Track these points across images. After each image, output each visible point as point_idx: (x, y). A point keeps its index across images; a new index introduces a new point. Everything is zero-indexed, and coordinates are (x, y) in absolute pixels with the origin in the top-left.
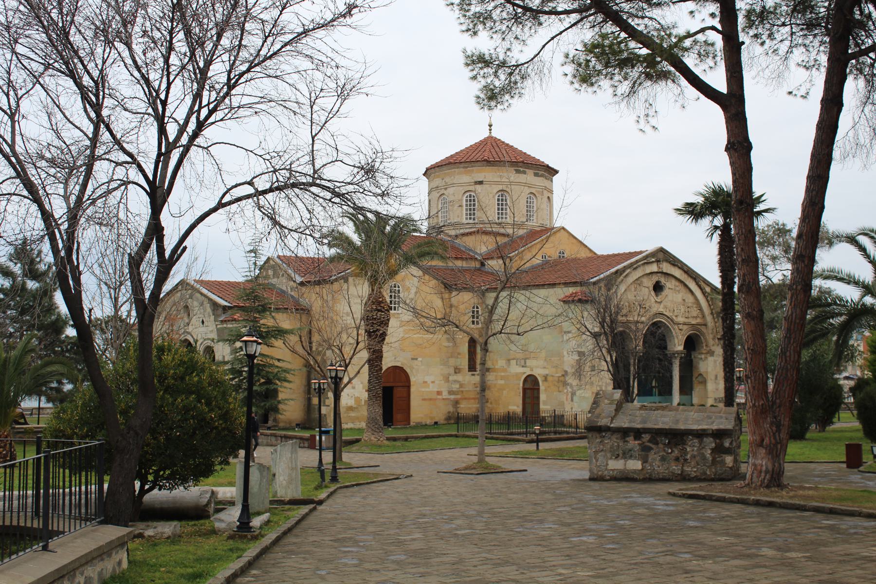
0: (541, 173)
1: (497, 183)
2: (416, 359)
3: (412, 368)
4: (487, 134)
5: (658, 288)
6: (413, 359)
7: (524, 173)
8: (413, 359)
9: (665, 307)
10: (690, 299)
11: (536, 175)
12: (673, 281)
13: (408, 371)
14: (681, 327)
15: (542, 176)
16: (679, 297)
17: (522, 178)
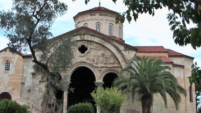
0: (103, 14)
1: (84, 21)
2: (15, 89)
3: (12, 93)
4: (99, 6)
5: (83, 49)
6: (13, 89)
7: (95, 15)
8: (13, 89)
9: (88, 59)
10: (108, 54)
11: (100, 15)
12: (95, 45)
13: (10, 94)
14: (99, 69)
15: (104, 15)
16: (100, 53)
17: (93, 17)
